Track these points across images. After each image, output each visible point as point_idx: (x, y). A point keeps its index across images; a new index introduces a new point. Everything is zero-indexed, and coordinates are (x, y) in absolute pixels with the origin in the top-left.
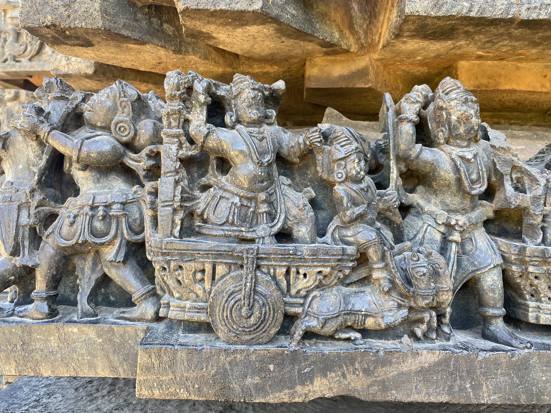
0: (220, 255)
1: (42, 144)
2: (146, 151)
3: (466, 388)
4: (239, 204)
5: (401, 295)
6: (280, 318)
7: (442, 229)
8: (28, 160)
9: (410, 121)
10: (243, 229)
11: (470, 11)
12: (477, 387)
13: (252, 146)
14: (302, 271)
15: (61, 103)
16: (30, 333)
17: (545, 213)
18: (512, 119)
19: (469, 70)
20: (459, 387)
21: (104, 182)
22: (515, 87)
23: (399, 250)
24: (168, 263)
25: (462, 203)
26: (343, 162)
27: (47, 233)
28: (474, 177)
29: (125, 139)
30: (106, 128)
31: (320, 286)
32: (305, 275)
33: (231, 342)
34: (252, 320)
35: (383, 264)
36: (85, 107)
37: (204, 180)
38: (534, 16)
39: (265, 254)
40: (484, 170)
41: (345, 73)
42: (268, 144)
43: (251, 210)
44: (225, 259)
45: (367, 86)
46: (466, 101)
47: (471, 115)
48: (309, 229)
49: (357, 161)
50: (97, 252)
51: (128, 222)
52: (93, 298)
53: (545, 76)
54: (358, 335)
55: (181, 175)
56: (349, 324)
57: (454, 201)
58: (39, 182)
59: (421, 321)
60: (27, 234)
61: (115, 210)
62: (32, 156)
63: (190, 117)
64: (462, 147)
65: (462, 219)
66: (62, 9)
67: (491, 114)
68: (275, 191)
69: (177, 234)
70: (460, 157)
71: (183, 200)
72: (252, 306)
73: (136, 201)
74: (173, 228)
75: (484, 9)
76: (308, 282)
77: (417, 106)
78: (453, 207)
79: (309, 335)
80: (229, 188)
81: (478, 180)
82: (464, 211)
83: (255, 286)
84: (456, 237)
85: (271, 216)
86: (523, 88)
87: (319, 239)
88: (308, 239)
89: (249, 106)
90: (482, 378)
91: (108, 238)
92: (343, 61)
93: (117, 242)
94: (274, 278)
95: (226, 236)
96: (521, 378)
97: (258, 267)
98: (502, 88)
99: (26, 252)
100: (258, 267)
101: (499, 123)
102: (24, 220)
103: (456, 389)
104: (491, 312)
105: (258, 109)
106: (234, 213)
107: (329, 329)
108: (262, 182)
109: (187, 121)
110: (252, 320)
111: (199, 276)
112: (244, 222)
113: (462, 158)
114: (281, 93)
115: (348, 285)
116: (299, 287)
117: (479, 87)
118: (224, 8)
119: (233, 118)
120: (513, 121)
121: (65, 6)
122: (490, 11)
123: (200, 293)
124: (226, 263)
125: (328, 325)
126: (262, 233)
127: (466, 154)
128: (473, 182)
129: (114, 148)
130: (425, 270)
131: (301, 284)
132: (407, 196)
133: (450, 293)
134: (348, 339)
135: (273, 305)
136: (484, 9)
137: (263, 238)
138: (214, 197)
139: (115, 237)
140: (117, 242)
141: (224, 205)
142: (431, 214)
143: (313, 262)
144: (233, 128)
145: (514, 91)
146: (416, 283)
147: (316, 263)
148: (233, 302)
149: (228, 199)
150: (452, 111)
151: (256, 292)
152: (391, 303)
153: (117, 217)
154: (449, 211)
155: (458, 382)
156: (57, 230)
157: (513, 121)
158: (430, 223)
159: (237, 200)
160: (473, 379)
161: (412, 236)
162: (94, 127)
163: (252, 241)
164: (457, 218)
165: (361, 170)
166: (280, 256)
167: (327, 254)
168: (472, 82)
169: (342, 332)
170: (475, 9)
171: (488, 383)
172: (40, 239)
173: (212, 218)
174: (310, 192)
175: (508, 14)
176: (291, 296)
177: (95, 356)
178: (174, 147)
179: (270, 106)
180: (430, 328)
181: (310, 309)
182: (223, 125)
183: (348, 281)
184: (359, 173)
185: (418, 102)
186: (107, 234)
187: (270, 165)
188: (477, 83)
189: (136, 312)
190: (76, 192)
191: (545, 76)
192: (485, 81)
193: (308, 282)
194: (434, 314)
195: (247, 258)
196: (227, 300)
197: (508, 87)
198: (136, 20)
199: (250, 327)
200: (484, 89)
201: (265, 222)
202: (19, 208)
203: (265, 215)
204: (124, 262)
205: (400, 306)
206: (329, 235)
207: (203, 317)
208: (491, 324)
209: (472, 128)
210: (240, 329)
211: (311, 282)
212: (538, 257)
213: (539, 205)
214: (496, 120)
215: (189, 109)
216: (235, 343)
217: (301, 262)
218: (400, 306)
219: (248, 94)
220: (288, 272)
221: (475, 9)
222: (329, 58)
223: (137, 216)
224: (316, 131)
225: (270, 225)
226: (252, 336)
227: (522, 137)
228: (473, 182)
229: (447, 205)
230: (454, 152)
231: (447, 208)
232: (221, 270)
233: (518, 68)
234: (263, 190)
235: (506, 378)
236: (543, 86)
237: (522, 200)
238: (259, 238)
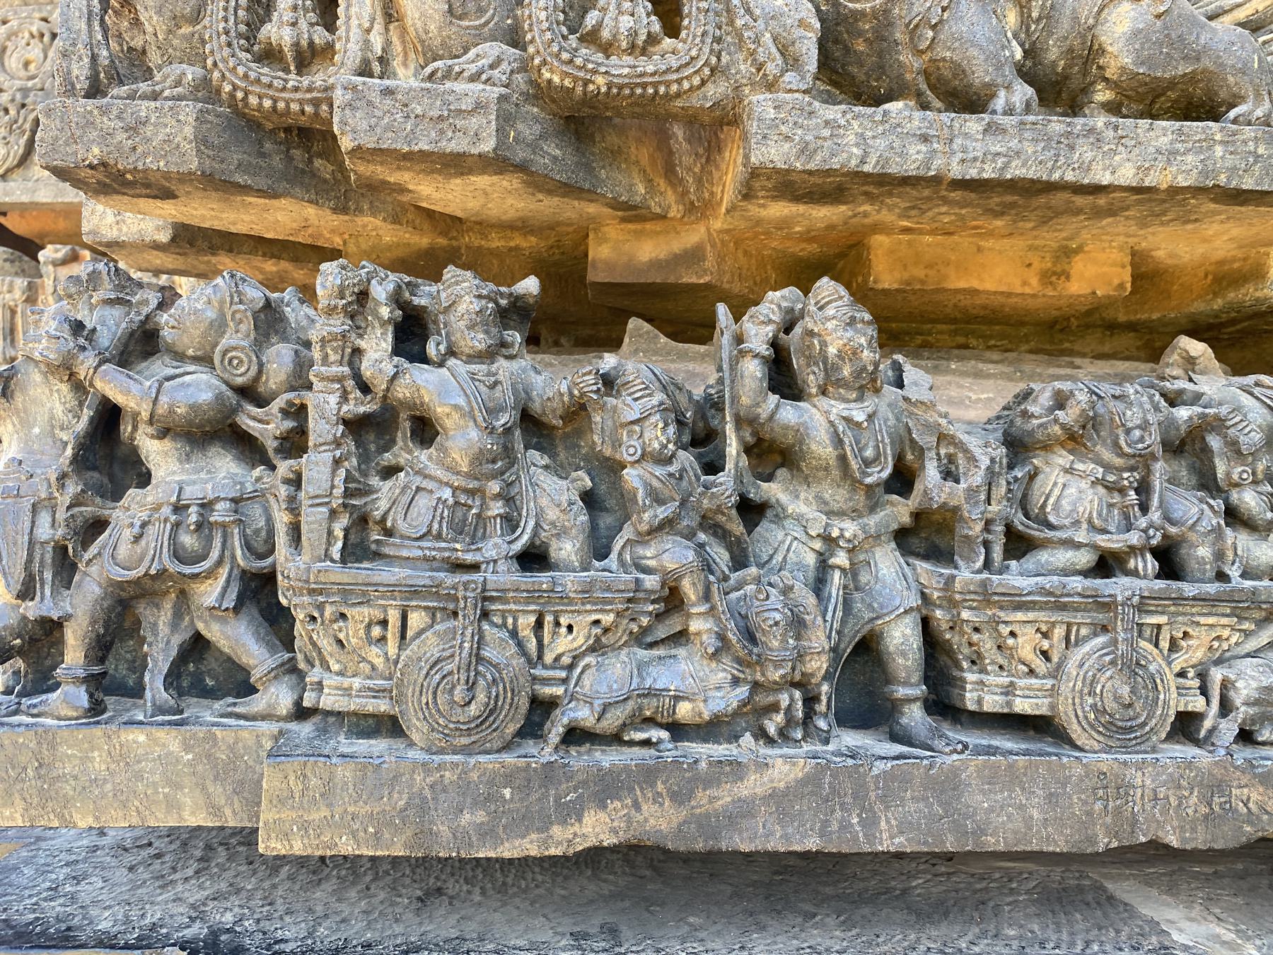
0: (415, 593)
1: (79, 388)
2: (279, 403)
3: (852, 825)
4: (451, 501)
5: (739, 661)
6: (524, 704)
7: (818, 545)
8: (52, 418)
9: (756, 356)
10: (458, 546)
11: (863, 162)
12: (870, 823)
13: (476, 398)
14: (564, 621)
15: (117, 312)
16: (53, 746)
17: (989, 516)
18: (991, 337)
19: (891, 252)
20: (841, 823)
21: (199, 460)
22: (975, 284)
23: (737, 582)
24: (321, 607)
25: (850, 499)
26: (637, 428)
27: (87, 556)
28: (869, 453)
29: (240, 381)
30: (205, 360)
32: (570, 628)
33: (434, 749)
34: (473, 709)
35: (708, 606)
36: (164, 318)
37: (388, 458)
38: (973, 173)
39: (497, 591)
40: (887, 441)
41: (662, 256)
42: (504, 395)
43: (474, 511)
44: (424, 599)
45: (702, 281)
46: (852, 322)
47: (861, 345)
48: (578, 545)
49: (661, 425)
50: (183, 594)
51: (244, 535)
52: (173, 679)
53: (1030, 265)
54: (664, 735)
55: (344, 449)
56: (648, 713)
57: (837, 495)
58: (75, 460)
59: (775, 707)
60: (48, 558)
61: (221, 513)
62: (59, 410)
63: (362, 344)
64: (848, 401)
65: (850, 528)
66: (121, 136)
67: (953, 327)
68: (518, 477)
69: (337, 556)
70: (844, 418)
71: (348, 493)
72: (474, 684)
73: (259, 496)
74: (329, 544)
75: (887, 160)
76: (574, 639)
77: (769, 330)
78: (836, 507)
79: (575, 736)
80: (432, 473)
81: (876, 459)
82: (855, 514)
83: (478, 648)
84: (841, 559)
85: (511, 523)
86: (989, 286)
87: (597, 564)
88: (576, 564)
89: (471, 327)
90: (878, 807)
91: (206, 565)
92: (658, 233)
93: (224, 572)
94: (514, 633)
95: (426, 559)
96: (945, 805)
97: (485, 615)
98: (952, 286)
99: (48, 592)
100: (485, 615)
101: (966, 347)
102: (44, 531)
103: (835, 826)
104: (901, 692)
105: (487, 332)
106: (442, 518)
107: (611, 722)
108: (494, 461)
109: (357, 352)
110: (473, 709)
111: (376, 631)
112: (461, 534)
113: (848, 420)
114: (531, 301)
115: (651, 646)
116: (560, 650)
117: (909, 284)
118: (426, 147)
119: (442, 348)
120: (992, 342)
121: (127, 129)
122: (897, 164)
123: (379, 662)
124: (426, 608)
125: (608, 715)
126: (492, 554)
127: (854, 413)
128: (867, 463)
129: (219, 397)
130: (778, 616)
131: (562, 645)
132: (759, 487)
133: (824, 658)
134: (647, 743)
135: (511, 681)
136: (887, 160)
137: (495, 561)
138: (405, 488)
139: (220, 562)
140: (224, 572)
141: (423, 502)
142: (799, 518)
143: (583, 604)
144: (441, 364)
145: (974, 292)
146: (763, 639)
147: (588, 607)
148: (438, 677)
149: (431, 492)
150: (828, 339)
151: (480, 659)
152: (721, 675)
153: (224, 526)
154: (829, 514)
155: (838, 814)
156: (108, 551)
157: (992, 342)
158: (796, 534)
159: (447, 494)
160: (863, 809)
161: (766, 558)
162: (180, 357)
163: (475, 567)
164: (843, 525)
165: (669, 441)
166: (525, 595)
167: (608, 589)
168: (897, 275)
169: (636, 729)
170: (872, 160)
171: (890, 815)
172: (73, 567)
173: (402, 526)
174: (583, 480)
175: (929, 169)
176: (545, 667)
177: (178, 786)
178: (333, 400)
179: (512, 323)
180: (790, 721)
181: (578, 689)
182: (424, 359)
183: (649, 639)
184: (666, 447)
185: (770, 321)
186: (204, 557)
187: (508, 431)
188: (906, 276)
189: (257, 703)
190: (144, 479)
191: (1030, 265)
192: (919, 272)
193: (574, 639)
194: (798, 694)
195: (465, 598)
196: (428, 673)
197: (962, 284)
198: (262, 155)
199: (469, 722)
200: (918, 287)
201: (499, 532)
202: (35, 509)
203: (498, 521)
204: (237, 610)
205: (736, 681)
206: (614, 556)
207: (383, 706)
208: (902, 714)
209: (864, 369)
210: (452, 726)
211: (581, 640)
212: (975, 593)
213: (977, 503)
214: (961, 340)
215: (360, 331)
216: (442, 751)
217: (563, 605)
218: (736, 681)
219: (469, 305)
220: (539, 624)
221: (872, 160)
222: (631, 226)
223: (262, 523)
224: (590, 373)
225: (508, 538)
226: (473, 738)
227: (994, 376)
228: (867, 463)
229: (826, 503)
230: (834, 410)
231: (827, 509)
232: (417, 620)
233: (979, 249)
234: (494, 476)
235: (921, 805)
236: (1025, 283)
237: (949, 494)
238: (488, 563)
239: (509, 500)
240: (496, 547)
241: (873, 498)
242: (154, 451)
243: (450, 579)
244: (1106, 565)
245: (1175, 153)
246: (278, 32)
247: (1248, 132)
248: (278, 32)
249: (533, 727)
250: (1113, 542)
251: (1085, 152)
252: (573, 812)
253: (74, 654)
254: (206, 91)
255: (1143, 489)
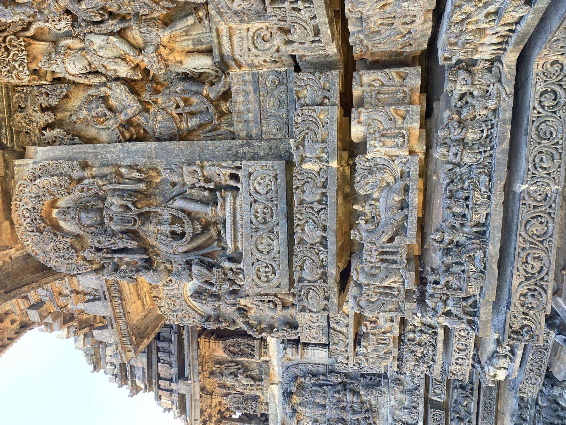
0: (467, 284)
31: (474, 265)
42: (444, 274)
57: (457, 235)
65: (461, 234)
73: (453, 298)
79: (484, 268)
85: (459, 274)
107: (483, 265)
131: (474, 269)
189: (478, 300)
190: (450, 310)
192: (420, 210)
219: (434, 277)
232: (470, 284)
239: (456, 274)
240: (462, 275)
241: (457, 230)
242: (447, 309)
243: (466, 281)
244: (467, 206)
245: (414, 194)
246: (396, 293)
247: (411, 184)
248: (396, 293)
249: (483, 273)
250: (465, 206)
251: (414, 205)
252: (493, 269)
253: (471, 318)
254: (403, 301)
255: (458, 201)
